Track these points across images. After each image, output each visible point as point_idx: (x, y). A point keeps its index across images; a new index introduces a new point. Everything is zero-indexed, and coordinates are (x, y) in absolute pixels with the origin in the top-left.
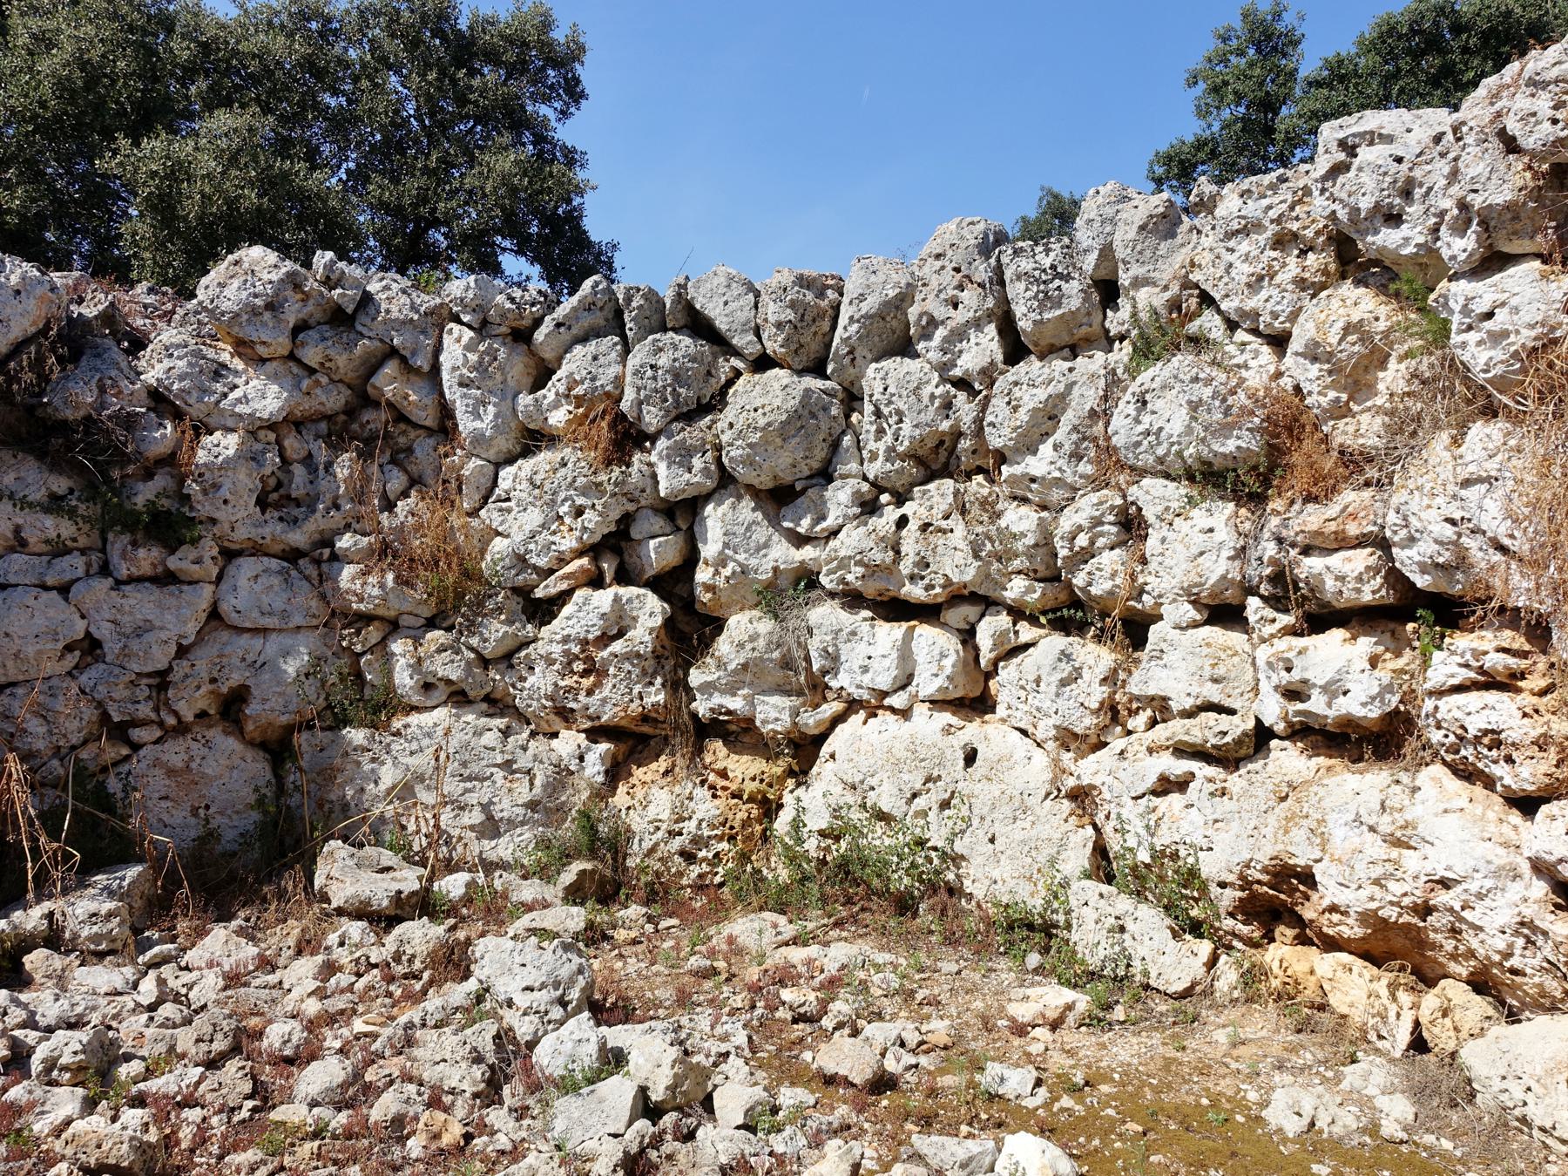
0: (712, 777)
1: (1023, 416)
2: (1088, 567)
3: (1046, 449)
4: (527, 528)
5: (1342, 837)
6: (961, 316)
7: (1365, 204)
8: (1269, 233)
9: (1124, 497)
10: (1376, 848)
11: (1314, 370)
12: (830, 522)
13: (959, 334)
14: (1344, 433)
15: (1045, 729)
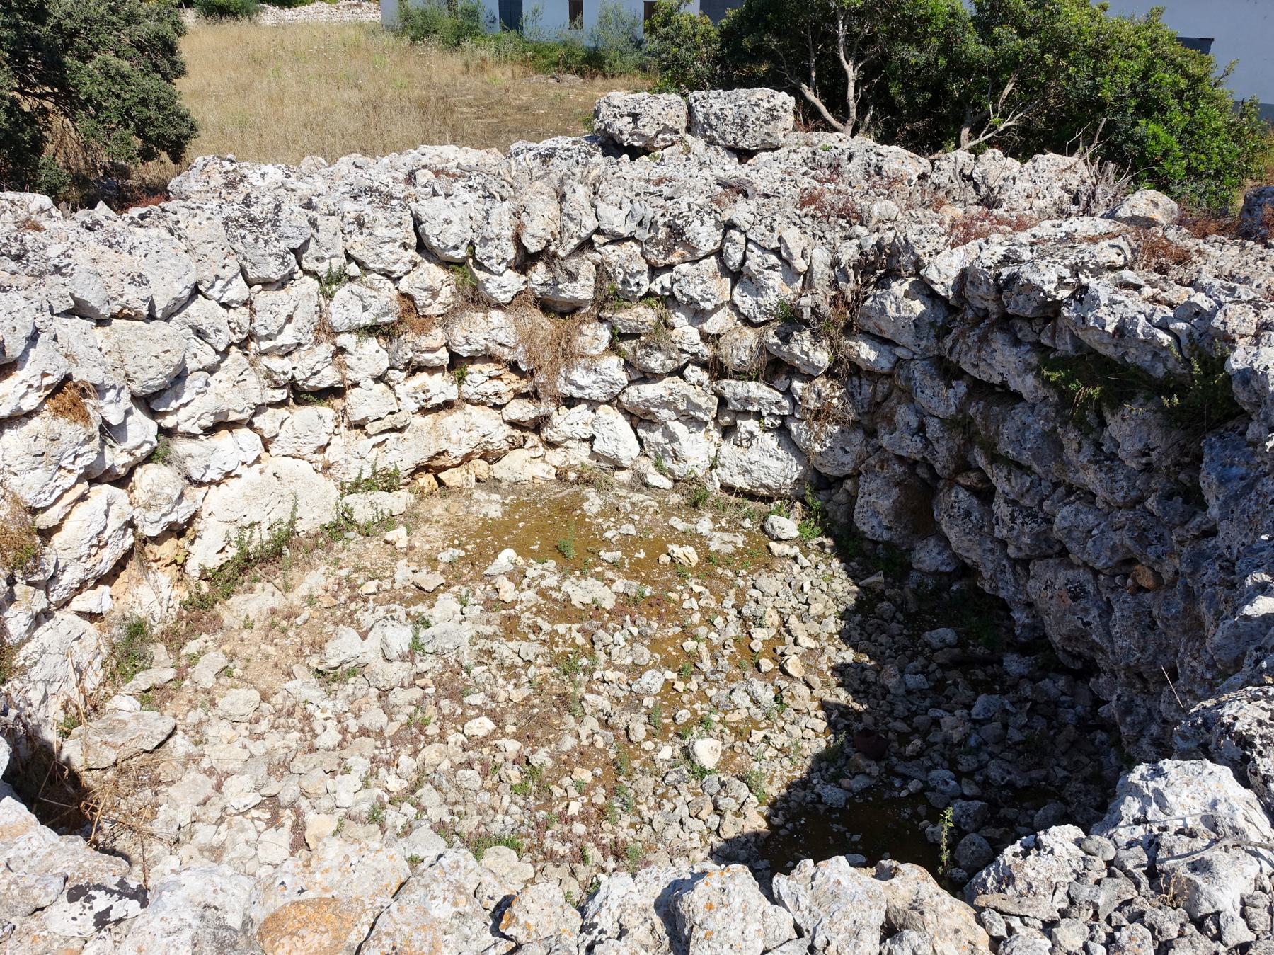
0: (154, 565)
1: (282, 319)
2: (319, 376)
3: (289, 329)
4: (38, 487)
5: (454, 437)
6: (227, 273)
7: (451, 244)
8: (398, 244)
9: (334, 344)
10: (466, 435)
11: (425, 293)
12: (184, 400)
13: (229, 282)
14: (428, 312)
15: (307, 450)
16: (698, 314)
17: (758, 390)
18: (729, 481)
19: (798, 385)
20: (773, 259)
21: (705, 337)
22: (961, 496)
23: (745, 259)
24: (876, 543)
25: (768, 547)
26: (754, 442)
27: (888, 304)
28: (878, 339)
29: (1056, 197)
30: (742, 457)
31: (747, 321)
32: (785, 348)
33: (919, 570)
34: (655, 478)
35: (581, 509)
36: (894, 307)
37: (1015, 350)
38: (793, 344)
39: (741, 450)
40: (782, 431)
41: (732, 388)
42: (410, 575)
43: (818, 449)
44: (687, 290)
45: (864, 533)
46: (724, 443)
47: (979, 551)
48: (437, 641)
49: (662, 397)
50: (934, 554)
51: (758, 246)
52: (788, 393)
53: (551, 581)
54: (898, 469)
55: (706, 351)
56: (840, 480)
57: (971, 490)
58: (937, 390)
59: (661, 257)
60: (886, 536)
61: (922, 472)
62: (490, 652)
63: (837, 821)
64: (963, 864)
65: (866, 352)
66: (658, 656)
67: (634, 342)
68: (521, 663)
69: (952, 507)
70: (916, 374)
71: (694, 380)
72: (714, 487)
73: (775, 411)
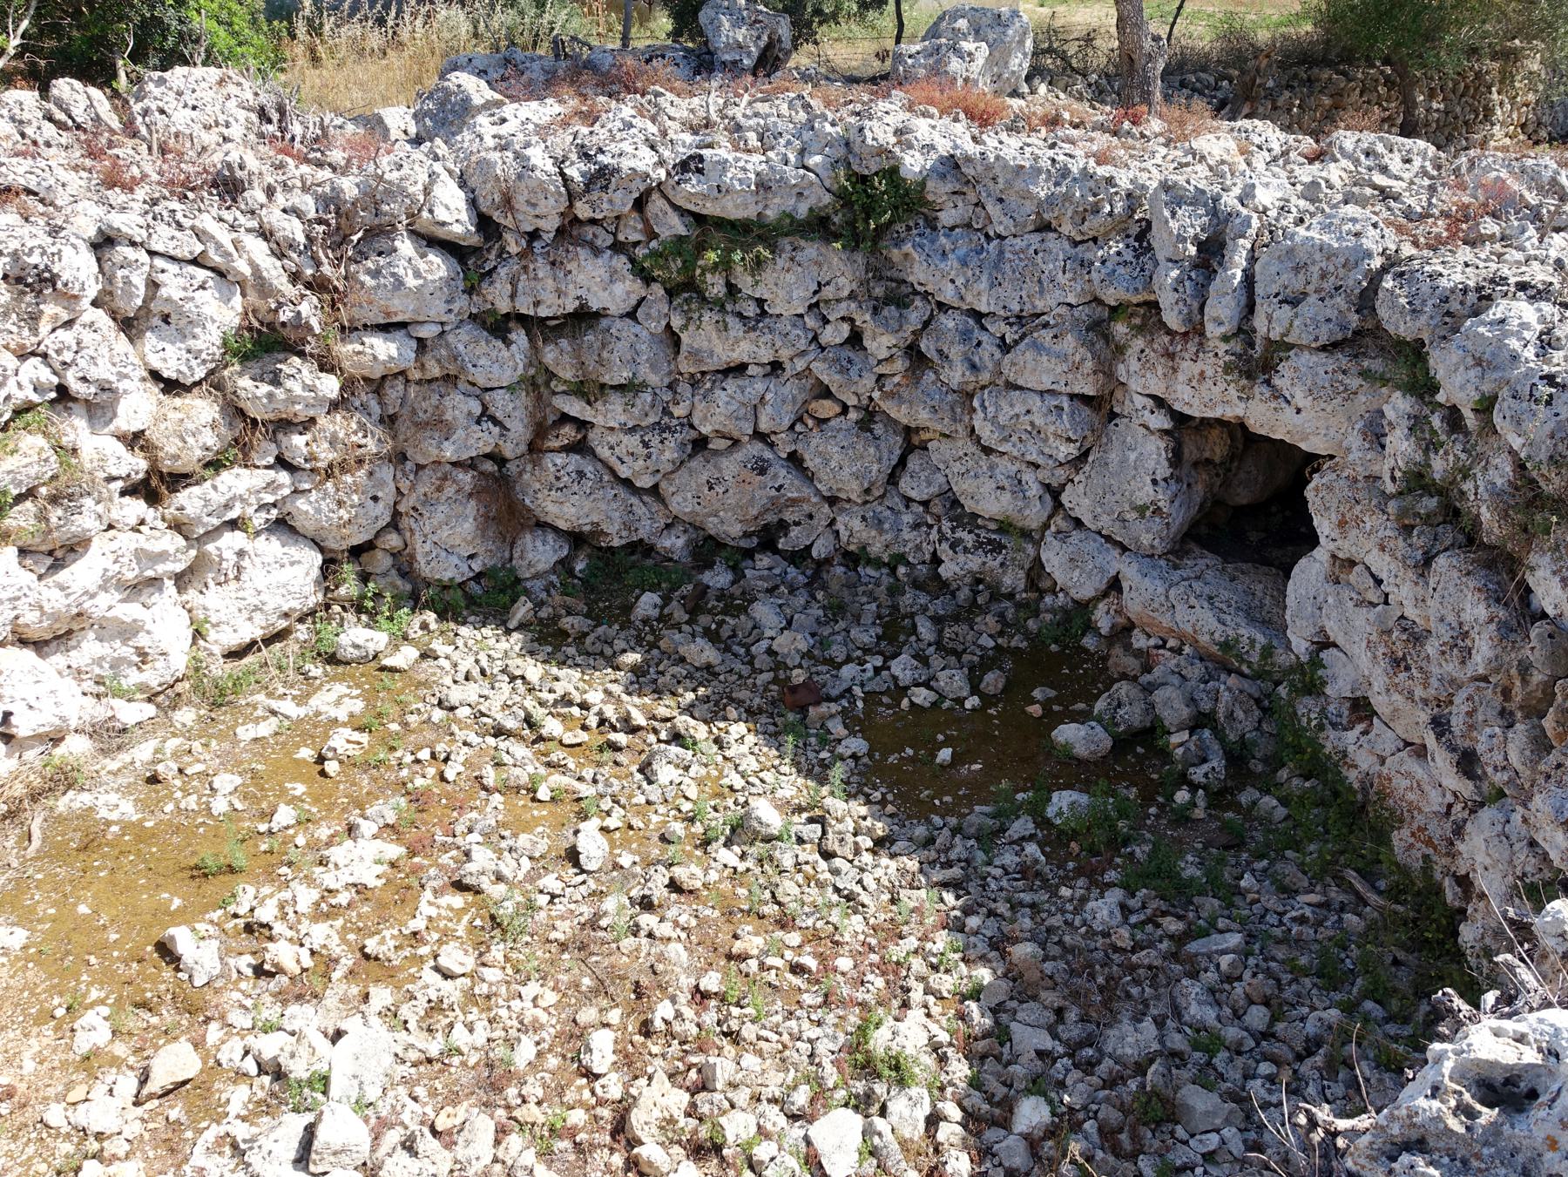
16: (100, 407)
17: (237, 482)
18: (234, 640)
19: (298, 442)
20: (202, 274)
21: (134, 440)
22: (559, 461)
23: (153, 285)
24: (462, 585)
25: (383, 669)
26: (246, 563)
27: (401, 272)
28: (386, 328)
29: (242, 120)
30: (240, 595)
31: (172, 387)
32: (280, 393)
33: (536, 576)
34: (133, 712)
35: (108, 823)
36: (410, 272)
37: (600, 261)
38: (289, 384)
39: (233, 585)
40: (283, 526)
41: (189, 500)
42: (117, 1102)
43: (346, 517)
44: (94, 373)
45: (451, 580)
46: (192, 595)
47: (603, 506)
48: (367, 1078)
49: (106, 570)
50: (541, 548)
51: (173, 259)
52: (282, 463)
53: (306, 897)
54: (466, 478)
55: (136, 465)
56: (369, 546)
57: (567, 449)
58: (494, 354)
59: (26, 332)
60: (477, 566)
61: (489, 466)
62: (435, 1007)
63: (885, 757)
64: (965, 694)
65: (384, 349)
66: (540, 829)
67: (28, 504)
68: (467, 981)
69: (558, 478)
70: (461, 347)
71: (133, 521)
72: (219, 669)
73: (270, 499)
